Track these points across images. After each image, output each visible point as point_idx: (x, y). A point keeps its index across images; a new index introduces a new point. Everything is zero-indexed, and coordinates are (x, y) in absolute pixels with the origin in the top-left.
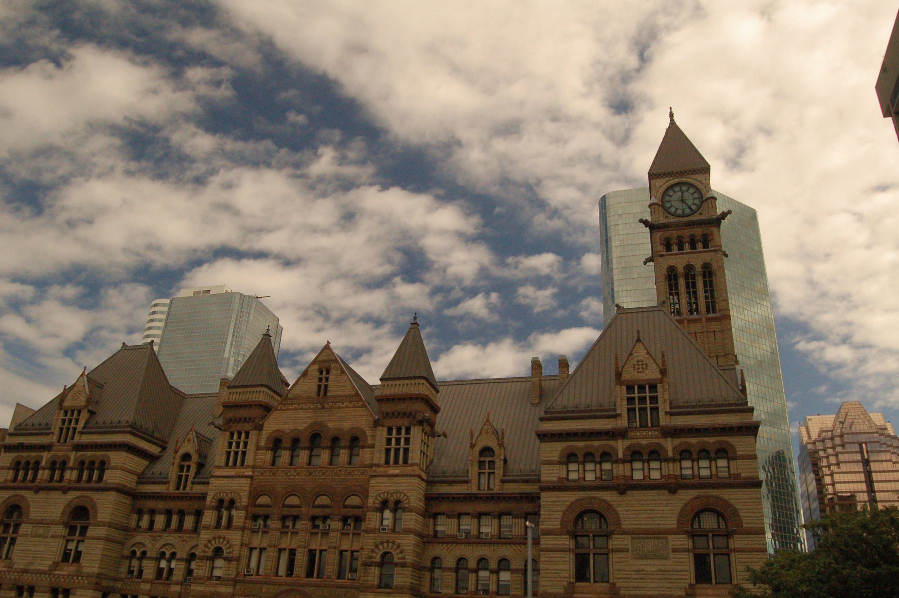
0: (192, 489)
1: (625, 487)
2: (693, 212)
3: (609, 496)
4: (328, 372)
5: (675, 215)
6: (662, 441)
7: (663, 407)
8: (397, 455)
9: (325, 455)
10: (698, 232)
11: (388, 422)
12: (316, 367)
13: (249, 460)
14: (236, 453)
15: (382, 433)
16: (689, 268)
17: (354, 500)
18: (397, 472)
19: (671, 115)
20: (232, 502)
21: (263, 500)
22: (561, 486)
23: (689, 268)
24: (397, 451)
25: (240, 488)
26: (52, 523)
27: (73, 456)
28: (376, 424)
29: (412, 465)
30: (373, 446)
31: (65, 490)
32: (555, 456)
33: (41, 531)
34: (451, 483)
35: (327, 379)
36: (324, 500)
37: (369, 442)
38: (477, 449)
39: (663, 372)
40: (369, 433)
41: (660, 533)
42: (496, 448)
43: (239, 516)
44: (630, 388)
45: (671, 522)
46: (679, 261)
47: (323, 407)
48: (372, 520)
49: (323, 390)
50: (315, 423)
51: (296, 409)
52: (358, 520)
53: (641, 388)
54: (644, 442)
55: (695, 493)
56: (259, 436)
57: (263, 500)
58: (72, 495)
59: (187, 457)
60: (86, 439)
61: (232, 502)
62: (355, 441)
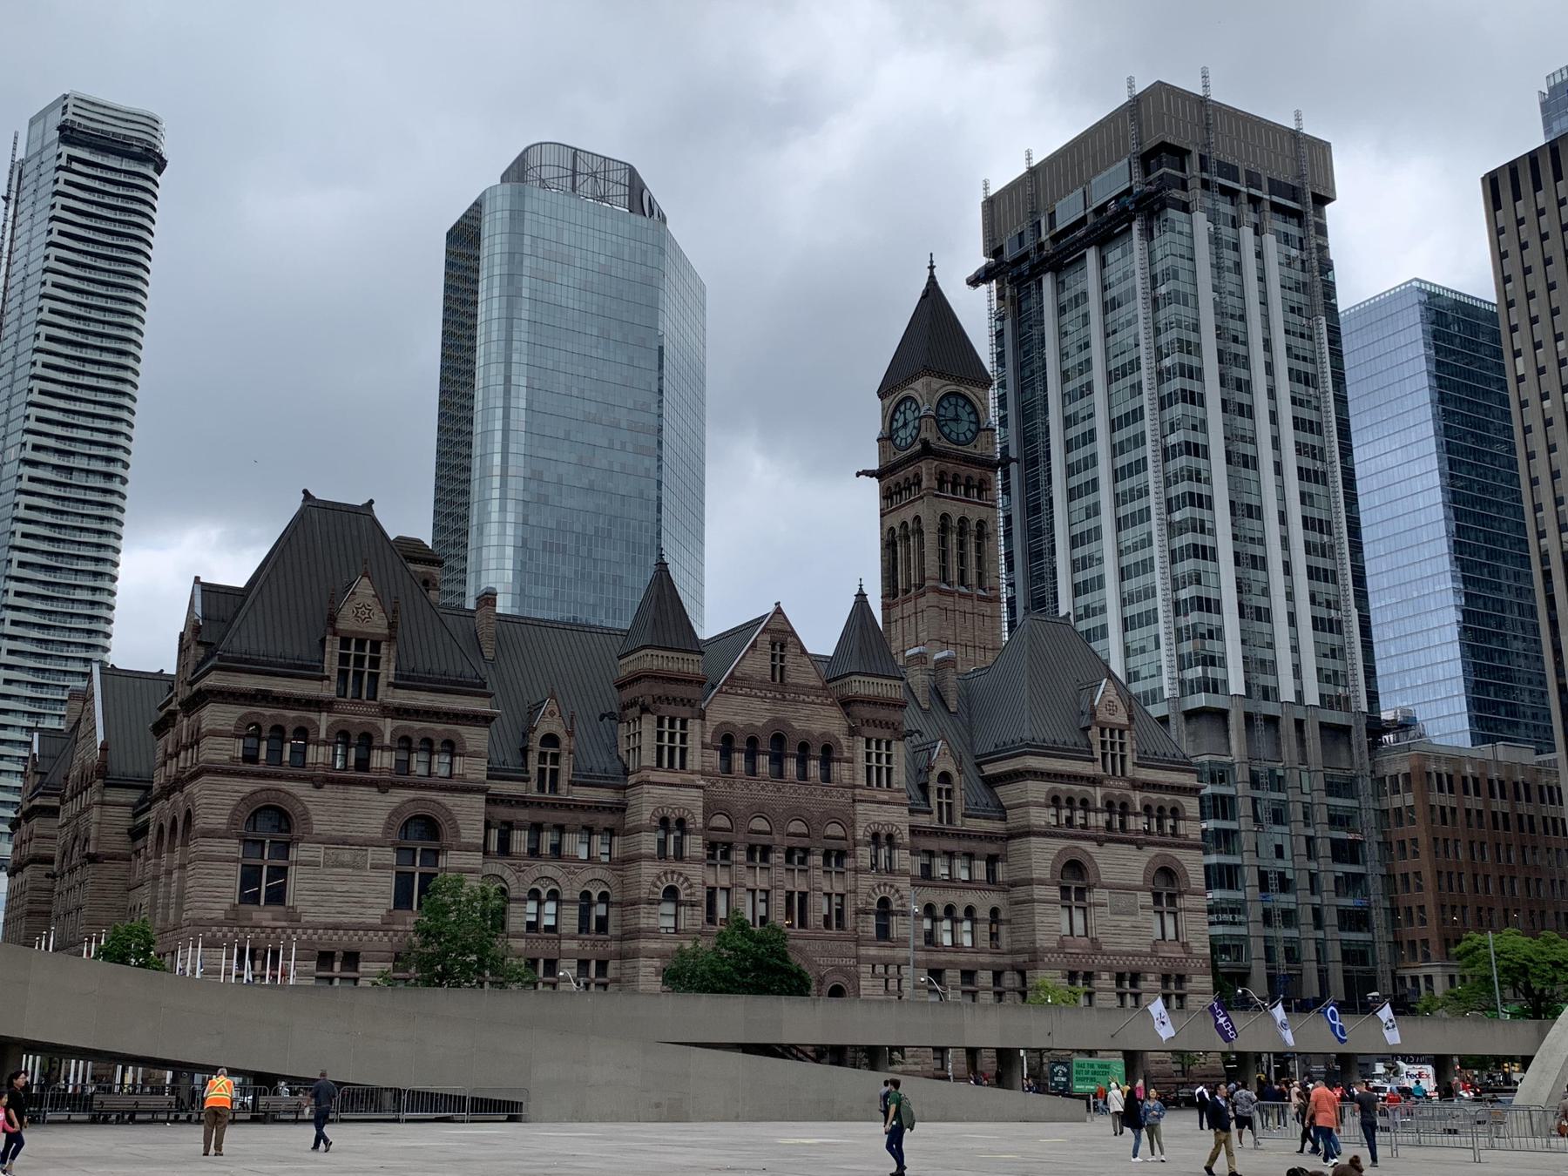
0: (569, 792)
2: (967, 443)
4: (782, 647)
5: (947, 437)
6: (1131, 793)
9: (791, 766)
10: (976, 473)
11: (868, 731)
12: (767, 637)
13: (695, 760)
14: (672, 750)
18: (885, 797)
19: (932, 268)
20: (681, 823)
24: (879, 770)
25: (690, 802)
27: (388, 727)
28: (853, 732)
29: (899, 791)
31: (383, 787)
33: (346, 856)
35: (782, 658)
36: (796, 827)
39: (1131, 718)
40: (844, 742)
41: (1129, 889)
43: (694, 845)
45: (1138, 880)
46: (956, 510)
47: (784, 698)
48: (864, 855)
49: (778, 671)
50: (775, 720)
51: (746, 695)
52: (841, 855)
54: (1117, 792)
55: (1156, 850)
57: (720, 821)
58: (398, 797)
59: (551, 740)
60: (403, 698)
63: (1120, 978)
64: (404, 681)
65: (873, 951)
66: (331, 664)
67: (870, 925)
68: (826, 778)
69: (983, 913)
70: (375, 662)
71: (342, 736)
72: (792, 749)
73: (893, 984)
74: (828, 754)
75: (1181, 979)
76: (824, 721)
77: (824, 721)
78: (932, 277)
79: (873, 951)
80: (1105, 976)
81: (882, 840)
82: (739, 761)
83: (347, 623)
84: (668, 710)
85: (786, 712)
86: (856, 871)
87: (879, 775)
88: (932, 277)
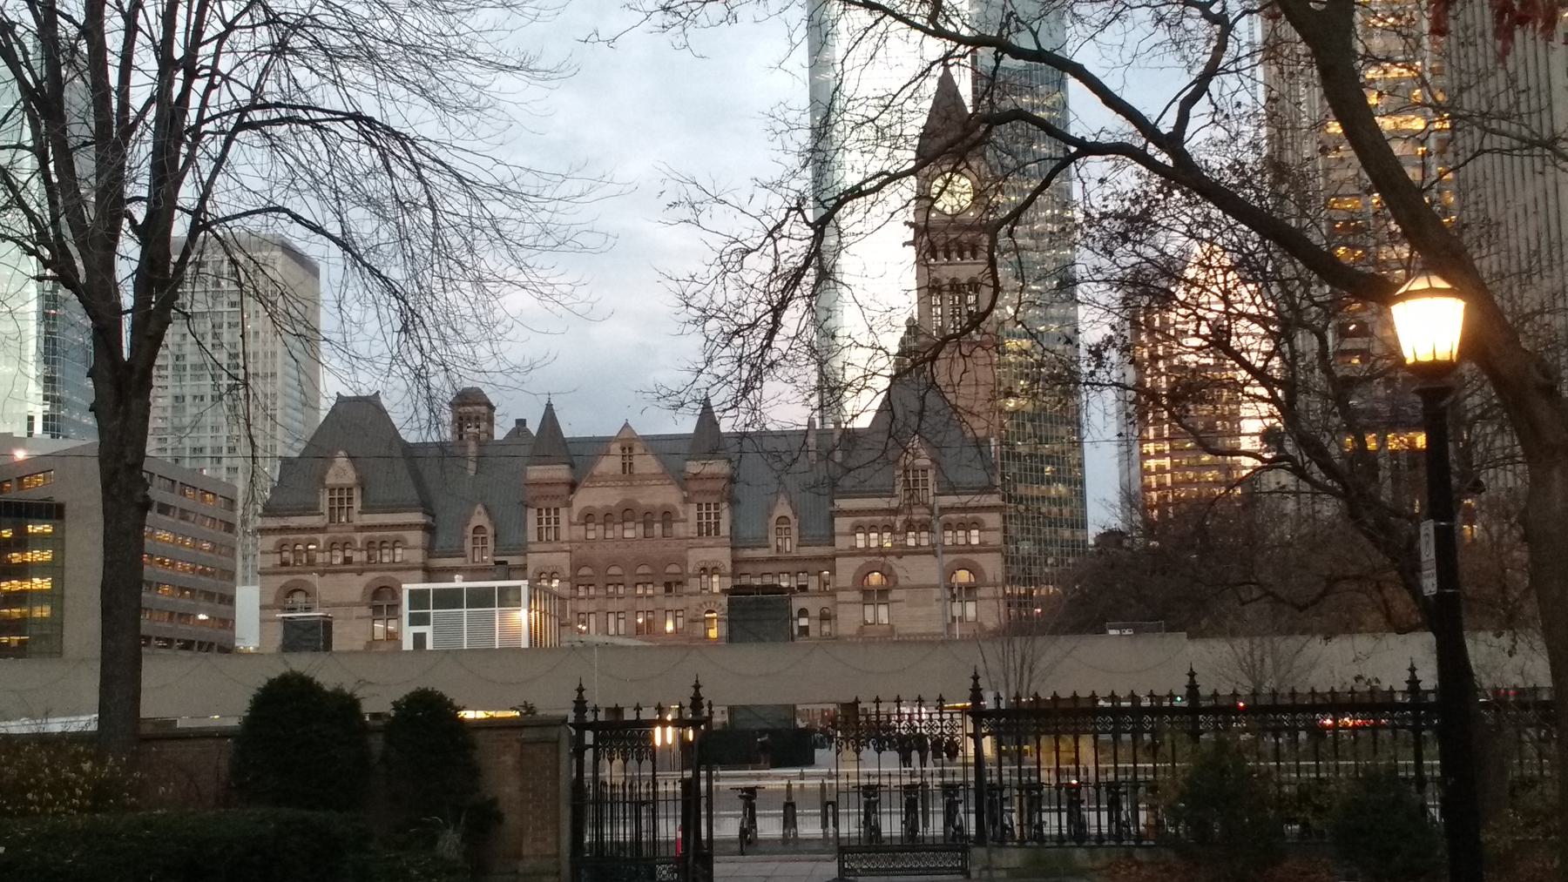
8: (708, 530)
13: (564, 535)
15: (693, 509)
21: (585, 571)
22: (854, 552)
27: (359, 538)
28: (686, 501)
30: (685, 521)
31: (360, 573)
32: (846, 529)
34: (753, 548)
37: (682, 516)
38: (775, 517)
40: (680, 508)
42: (791, 517)
48: (694, 585)
57: (585, 571)
58: (369, 577)
59: (478, 529)
60: (369, 519)
62: (668, 516)
64: (367, 509)
66: (324, 505)
69: (814, 612)
70: (350, 499)
76: (668, 496)
77: (668, 496)
84: (543, 504)
85: (631, 494)
86: (691, 594)
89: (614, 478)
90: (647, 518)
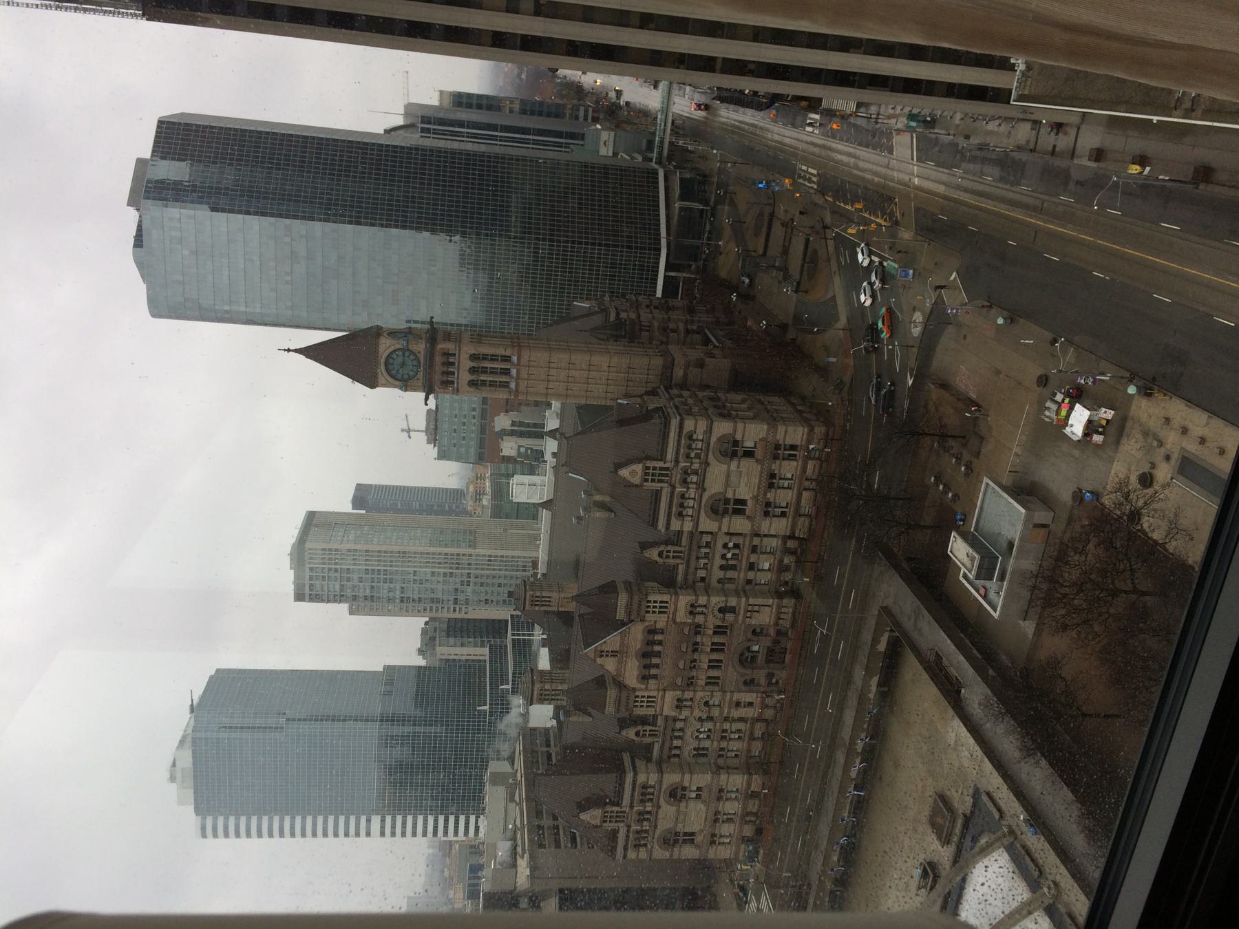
1: (701, 487)
2: (417, 359)
3: (706, 496)
7: (661, 464)
9: (657, 648)
10: (438, 359)
11: (643, 613)
16: (473, 370)
17: (686, 631)
19: (289, 350)
20: (678, 700)
23: (473, 370)
25: (670, 696)
26: (678, 810)
28: (643, 620)
31: (659, 807)
33: (682, 817)
44: (646, 480)
45: (725, 467)
46: (465, 377)
48: (700, 619)
53: (646, 474)
56: (640, 690)
59: (637, 734)
61: (678, 700)
62: (652, 631)
63: (771, 486)
65: (741, 618)
67: (730, 617)
68: (662, 632)
69: (727, 539)
71: (640, 821)
72: (649, 649)
73: (756, 608)
74: (652, 631)
75: (777, 447)
78: (296, 351)
79: (741, 618)
80: (769, 495)
81: (692, 610)
82: (653, 671)
83: (598, 822)
87: (663, 607)
88: (296, 351)
89: (620, 662)
90: (651, 643)
